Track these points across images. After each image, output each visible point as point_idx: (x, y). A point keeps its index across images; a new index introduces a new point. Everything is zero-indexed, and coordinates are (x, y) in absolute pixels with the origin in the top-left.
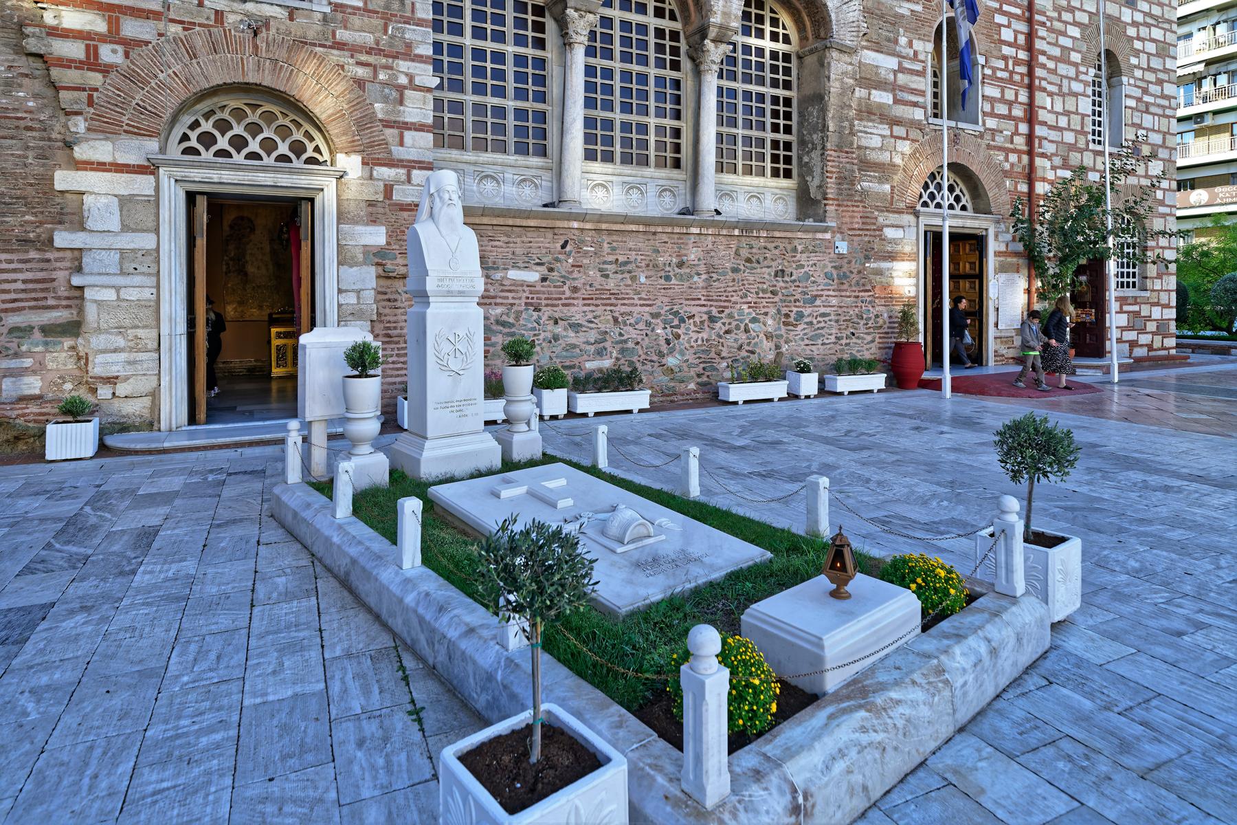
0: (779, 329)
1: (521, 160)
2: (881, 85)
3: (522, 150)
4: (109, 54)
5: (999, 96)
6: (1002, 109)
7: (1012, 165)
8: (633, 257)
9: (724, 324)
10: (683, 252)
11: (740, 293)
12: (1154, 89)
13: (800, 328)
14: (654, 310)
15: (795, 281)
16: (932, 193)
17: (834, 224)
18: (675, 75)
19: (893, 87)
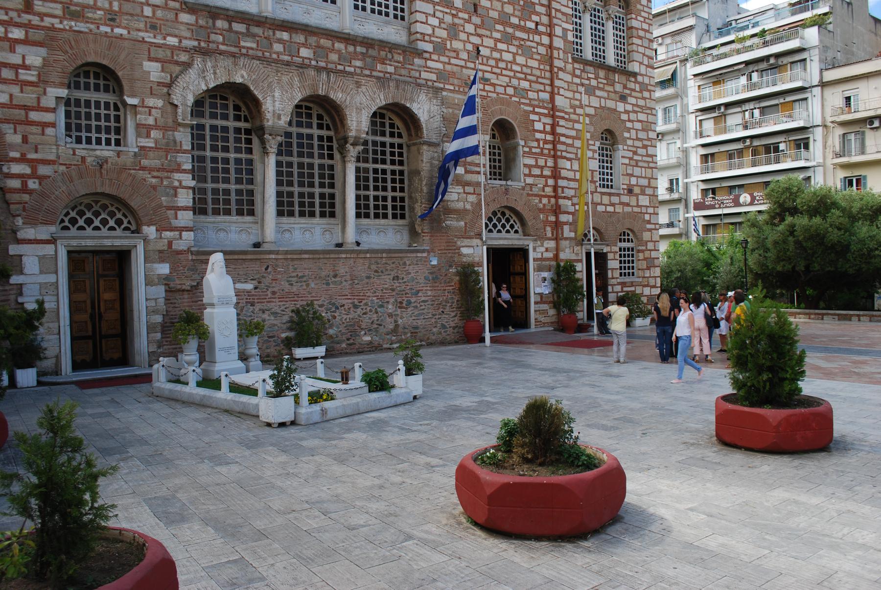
0: (396, 311)
1: (240, 218)
3: (240, 213)
4: (32, 184)
5: (534, 163)
6: (537, 171)
7: (544, 205)
8: (307, 272)
9: (362, 309)
10: (336, 268)
11: (372, 291)
12: (642, 151)
13: (409, 309)
14: (320, 303)
15: (405, 282)
16: (495, 224)
17: (428, 248)
18: (330, 162)
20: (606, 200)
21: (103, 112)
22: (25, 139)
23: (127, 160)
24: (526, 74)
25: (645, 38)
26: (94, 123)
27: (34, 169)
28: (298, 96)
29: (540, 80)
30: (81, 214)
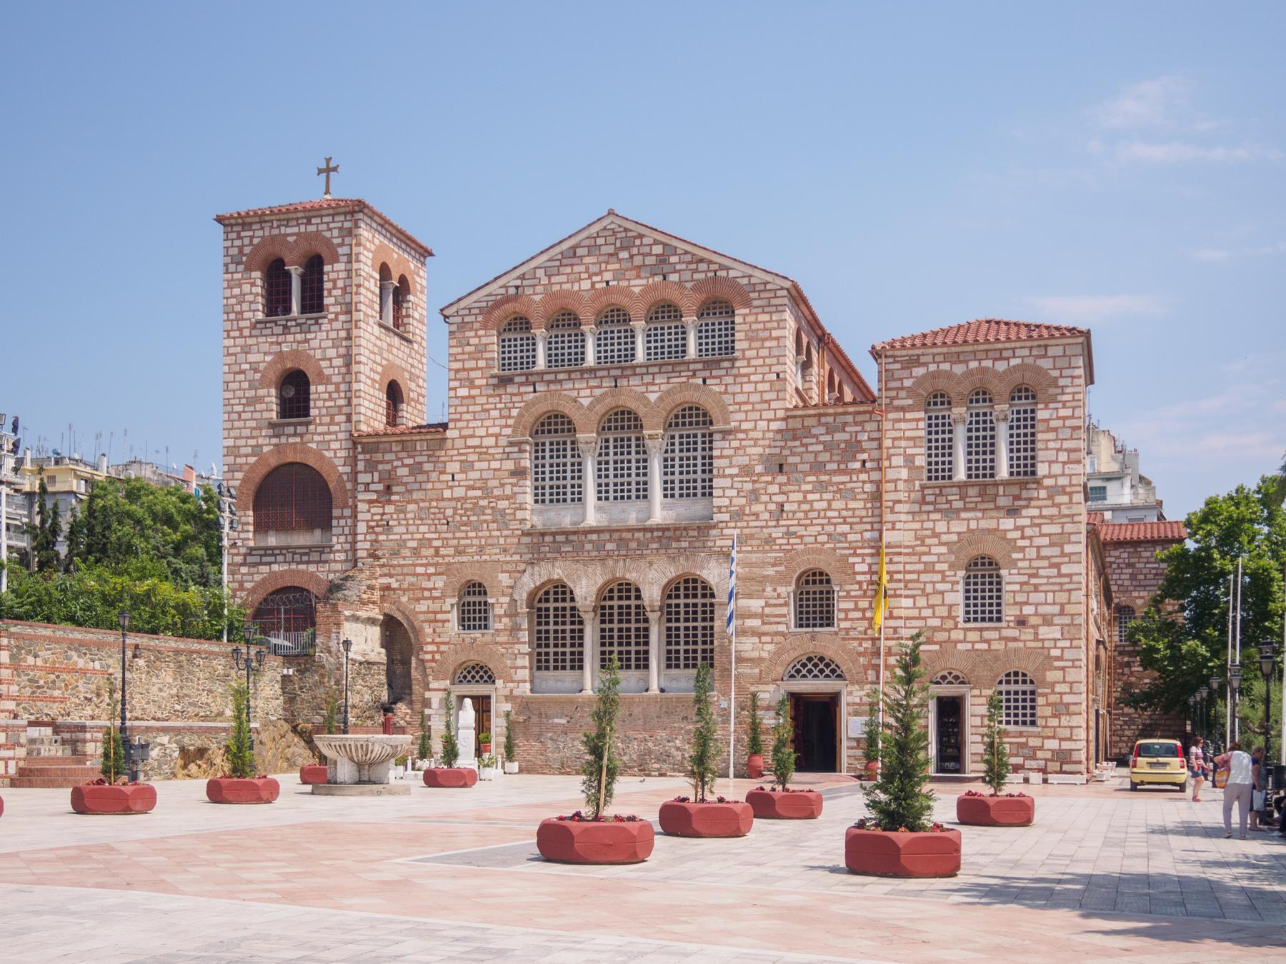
2: (752, 616)
3: (573, 668)
4: (437, 657)
6: (859, 615)
7: (866, 649)
19: (762, 616)
20: (973, 636)
21: (483, 608)
22: (434, 630)
23: (488, 638)
24: (845, 518)
25: (1064, 426)
26: (477, 615)
27: (438, 647)
28: (600, 582)
29: (865, 520)
30: (469, 672)
